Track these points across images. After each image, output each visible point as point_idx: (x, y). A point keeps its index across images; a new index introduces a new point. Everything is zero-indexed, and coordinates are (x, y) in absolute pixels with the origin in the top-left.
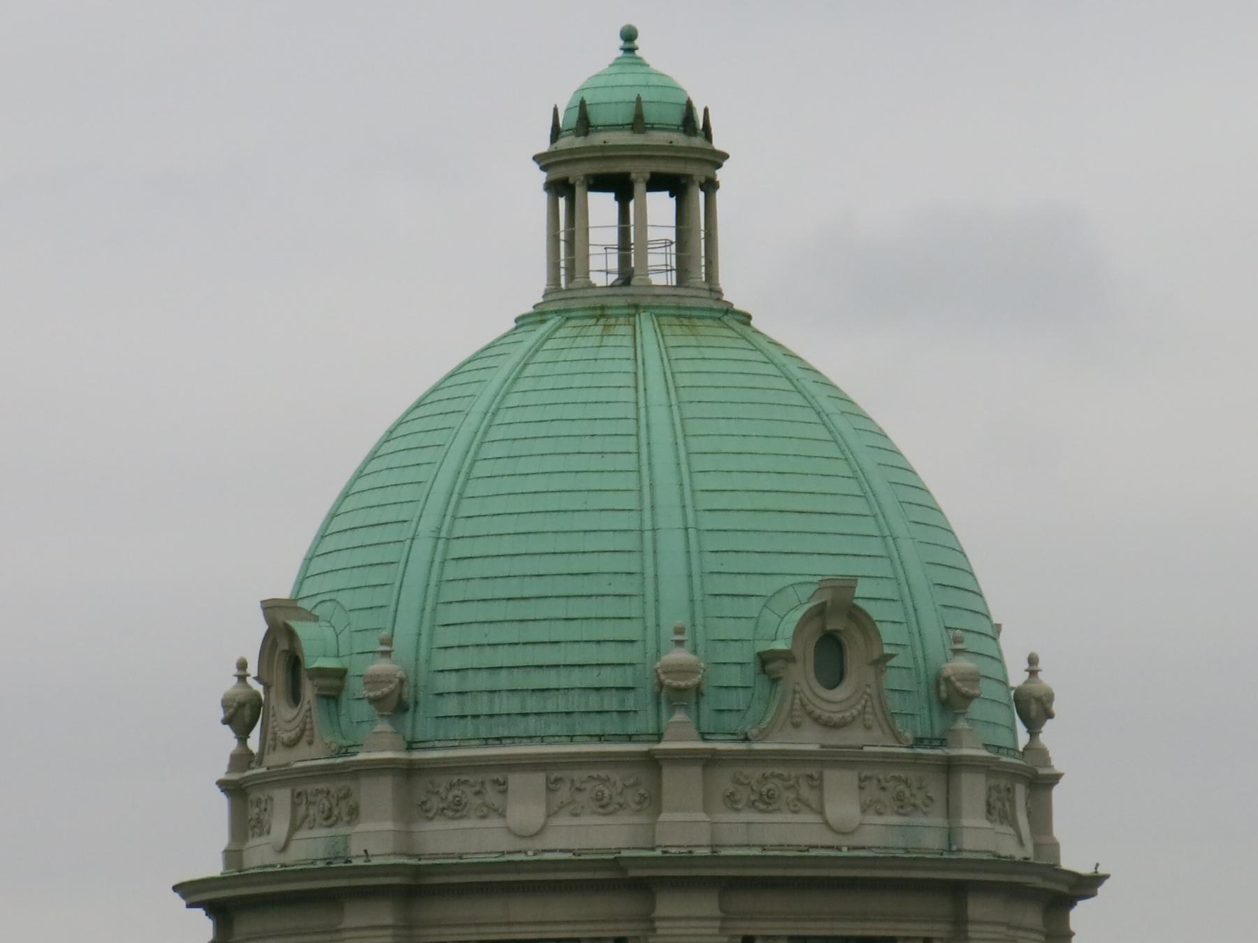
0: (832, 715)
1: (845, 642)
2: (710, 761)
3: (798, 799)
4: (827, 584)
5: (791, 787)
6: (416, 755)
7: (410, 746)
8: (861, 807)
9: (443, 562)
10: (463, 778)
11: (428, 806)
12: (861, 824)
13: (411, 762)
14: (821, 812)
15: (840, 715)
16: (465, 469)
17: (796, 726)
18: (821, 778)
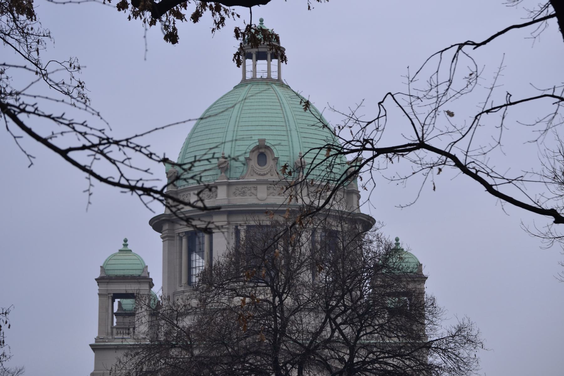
0: (261, 172)
1: (267, 155)
2: (229, 185)
3: (251, 193)
4: (260, 140)
5: (250, 190)
6: (230, 181)
7: (228, 179)
8: (267, 194)
9: (223, 137)
10: (245, 186)
11: (236, 193)
12: (267, 198)
13: (229, 182)
14: (257, 196)
15: (263, 172)
16: (239, 116)
17: (252, 175)
18: (257, 187)
